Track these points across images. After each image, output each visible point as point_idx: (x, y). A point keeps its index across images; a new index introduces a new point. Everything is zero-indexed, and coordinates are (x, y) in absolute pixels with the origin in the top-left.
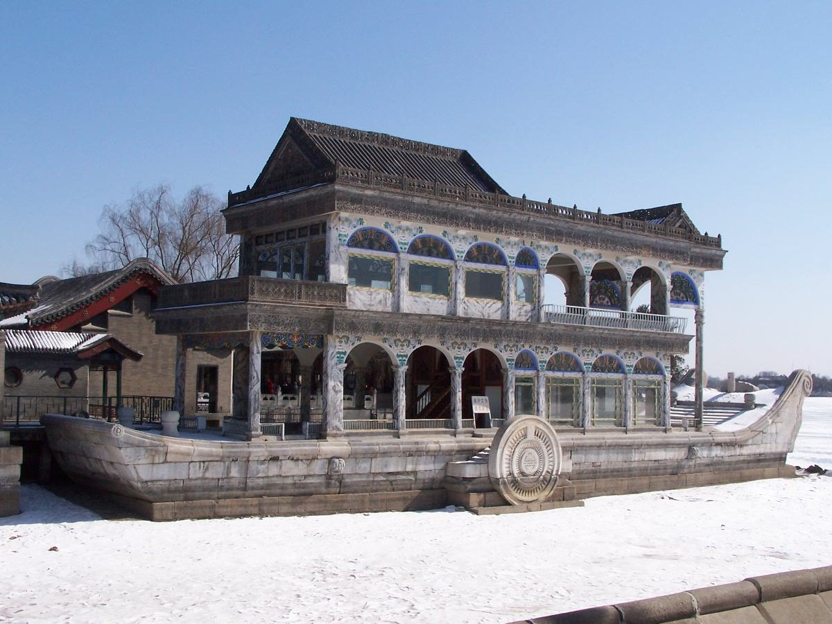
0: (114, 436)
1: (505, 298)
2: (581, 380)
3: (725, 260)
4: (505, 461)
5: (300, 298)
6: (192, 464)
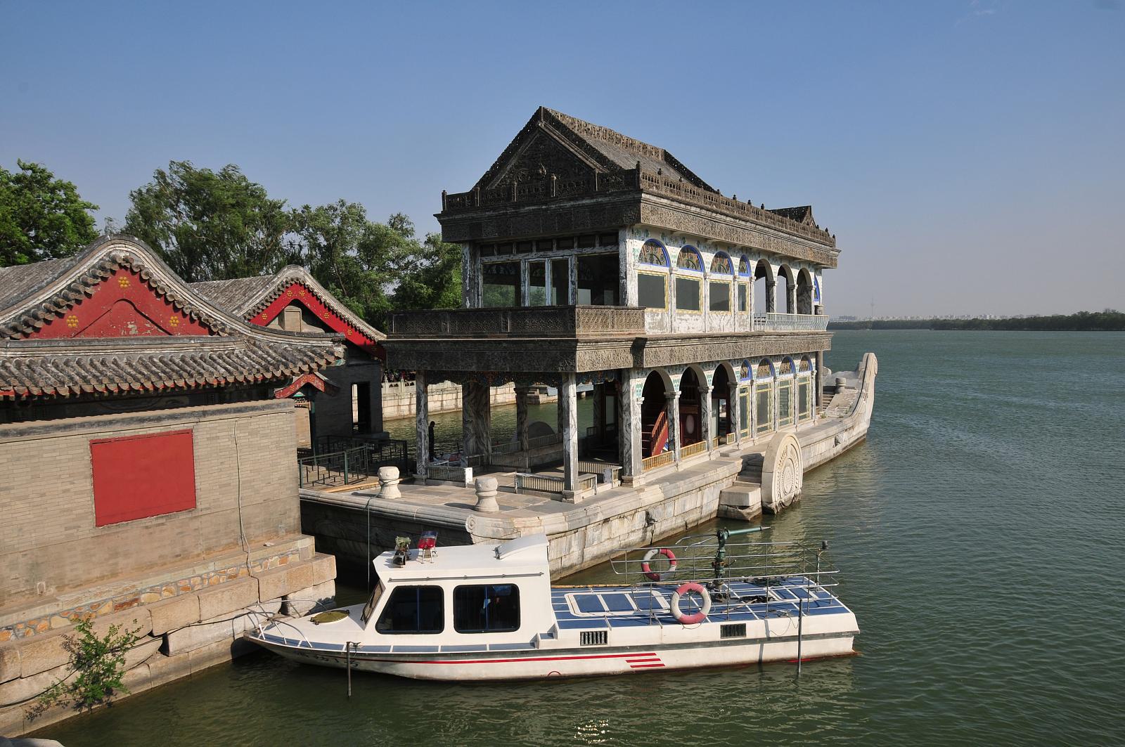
0: (468, 530)
1: (732, 308)
2: (772, 384)
4: (777, 482)
5: (613, 327)
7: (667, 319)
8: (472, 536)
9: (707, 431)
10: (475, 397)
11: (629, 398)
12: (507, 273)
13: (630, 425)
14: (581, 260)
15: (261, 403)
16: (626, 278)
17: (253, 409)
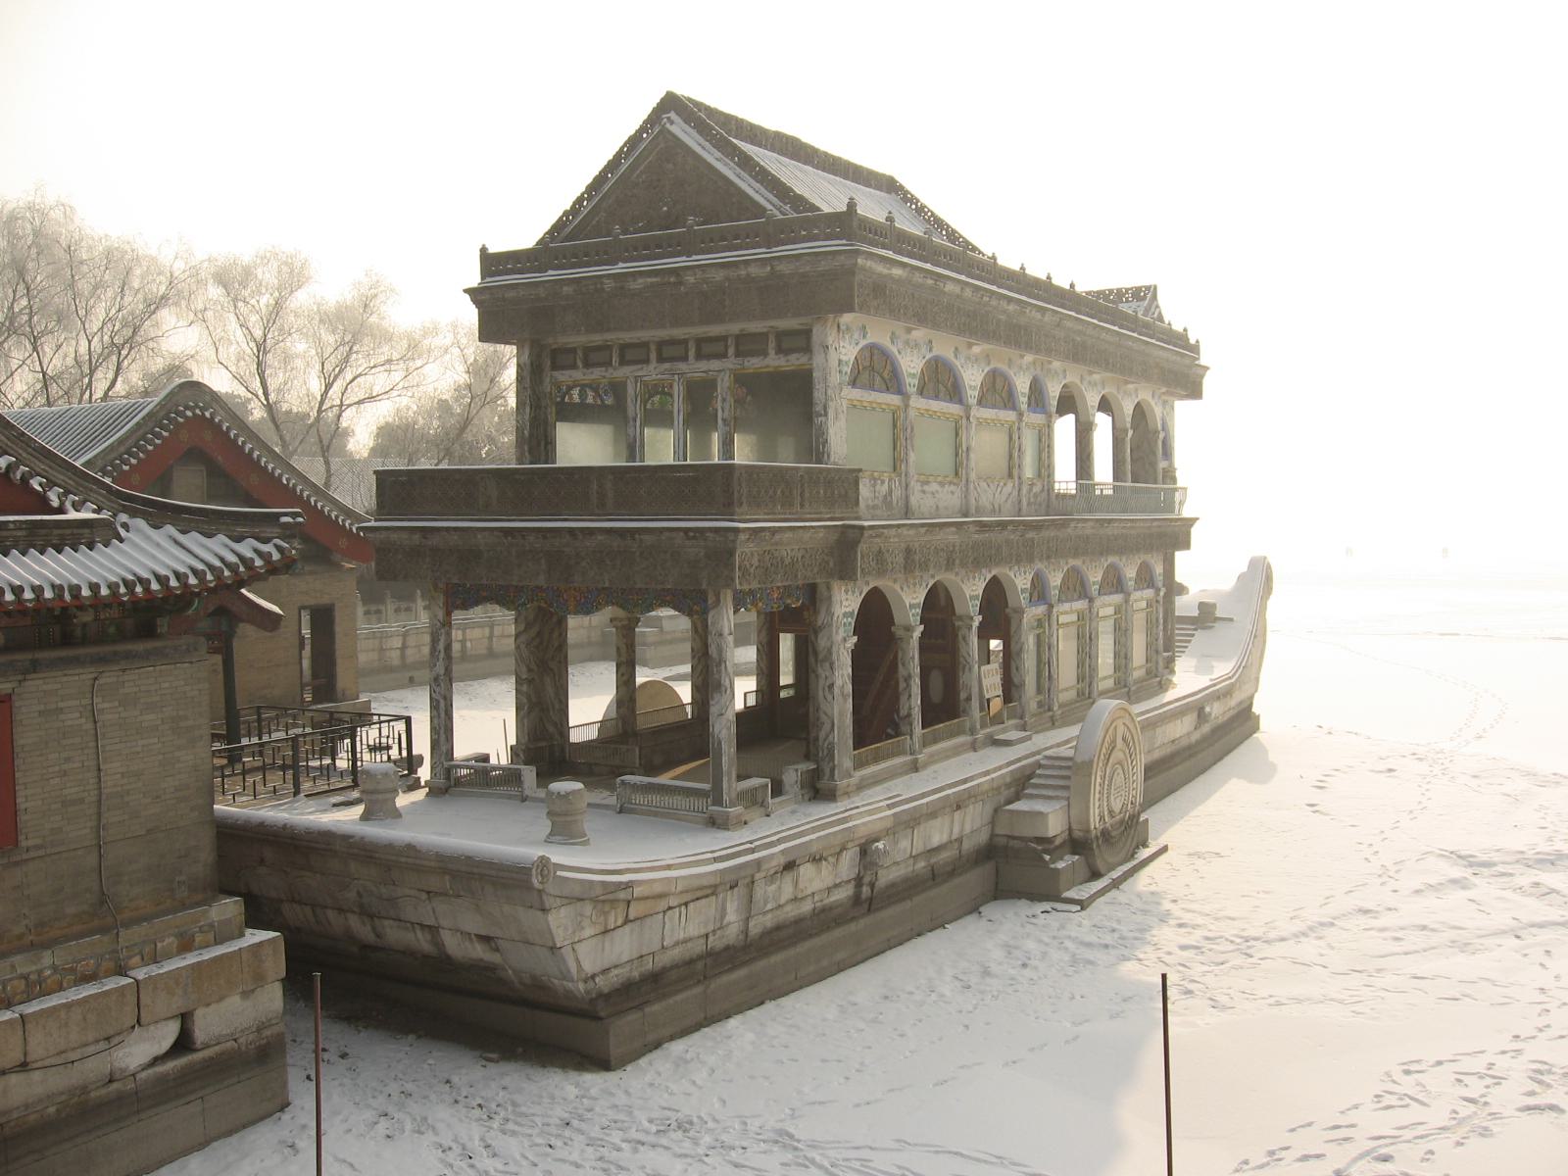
3: (1208, 383)
5: (802, 506)
6: (670, 912)
7: (897, 493)
8: (545, 897)
9: (969, 699)
10: (539, 634)
11: (830, 637)
12: (599, 402)
13: (831, 686)
14: (741, 379)
15: (140, 647)
16: (826, 415)
17: (128, 656)
